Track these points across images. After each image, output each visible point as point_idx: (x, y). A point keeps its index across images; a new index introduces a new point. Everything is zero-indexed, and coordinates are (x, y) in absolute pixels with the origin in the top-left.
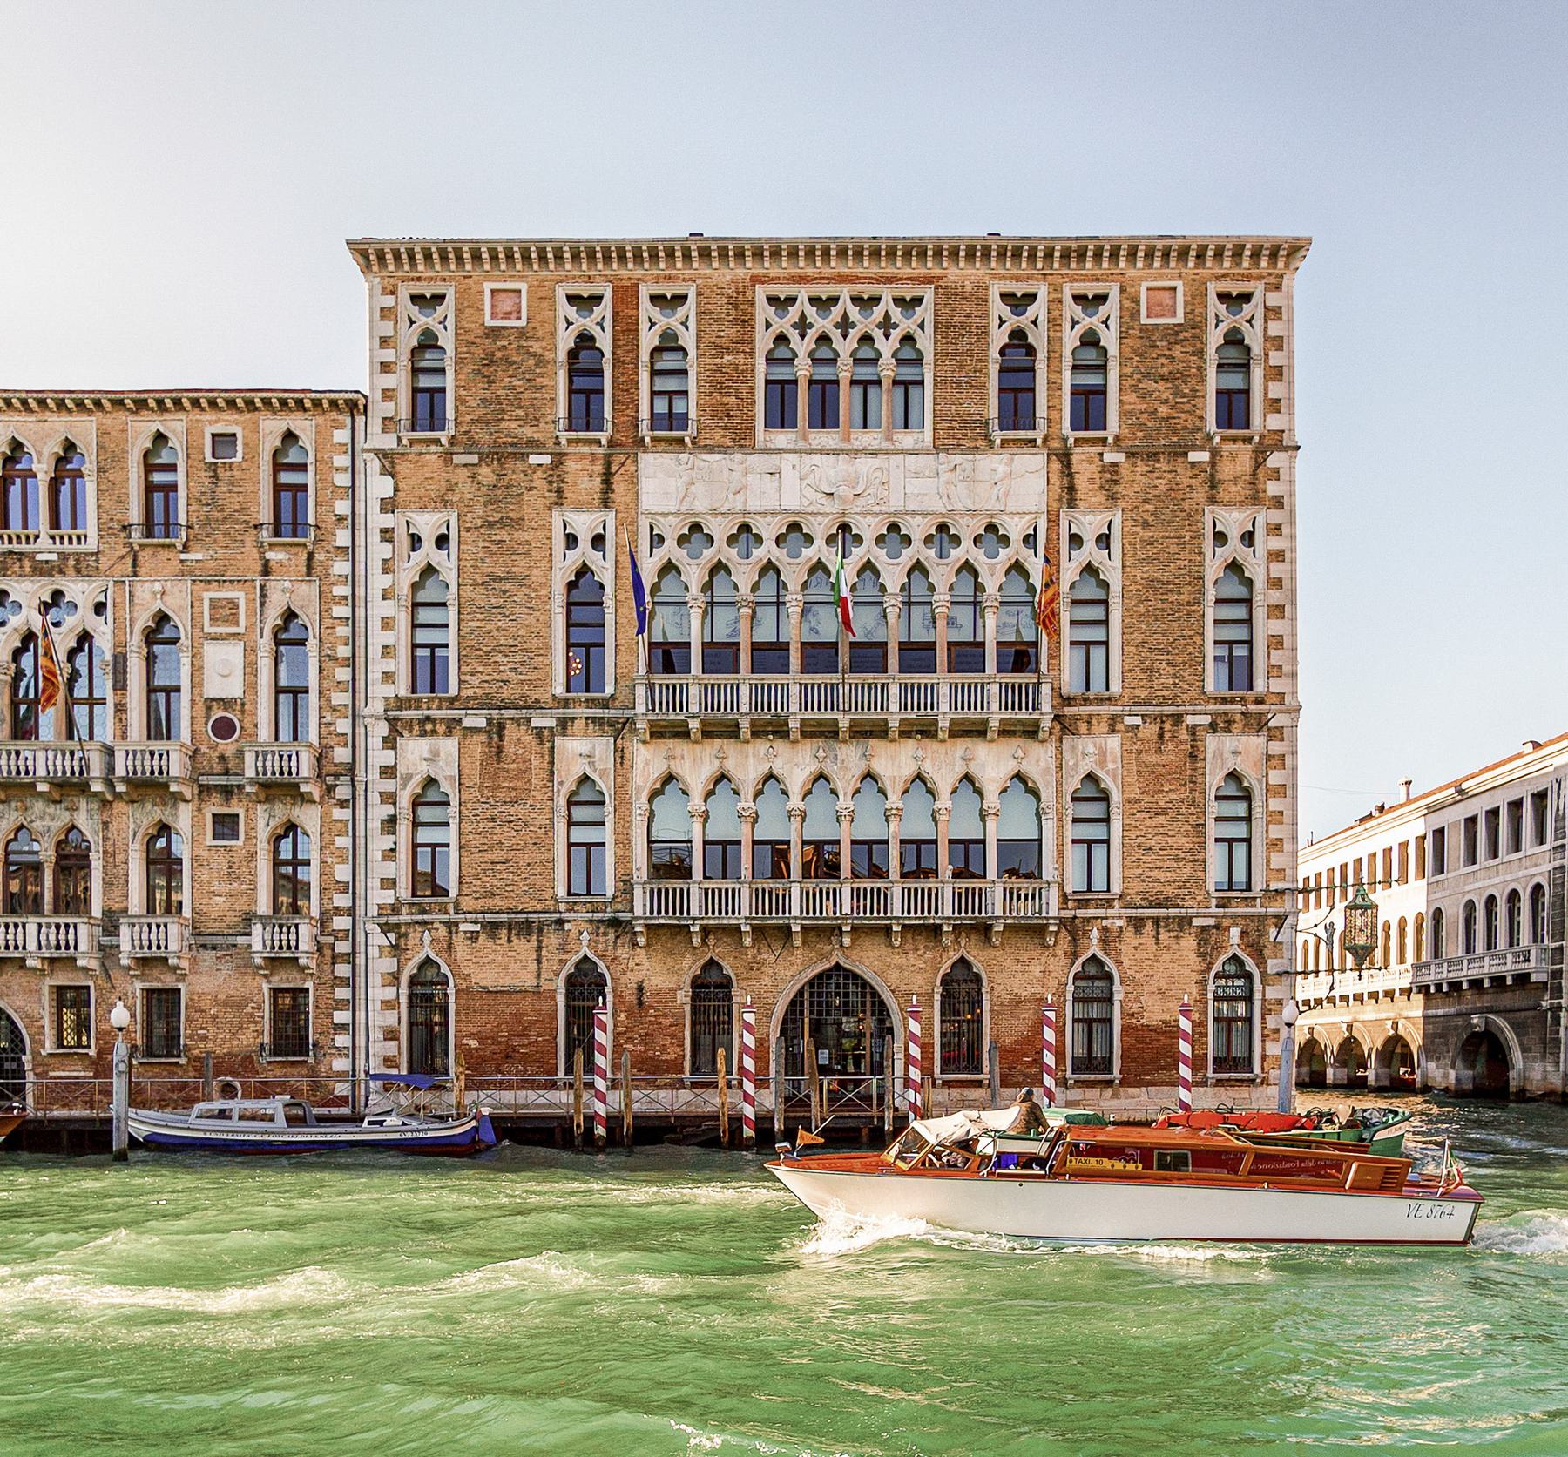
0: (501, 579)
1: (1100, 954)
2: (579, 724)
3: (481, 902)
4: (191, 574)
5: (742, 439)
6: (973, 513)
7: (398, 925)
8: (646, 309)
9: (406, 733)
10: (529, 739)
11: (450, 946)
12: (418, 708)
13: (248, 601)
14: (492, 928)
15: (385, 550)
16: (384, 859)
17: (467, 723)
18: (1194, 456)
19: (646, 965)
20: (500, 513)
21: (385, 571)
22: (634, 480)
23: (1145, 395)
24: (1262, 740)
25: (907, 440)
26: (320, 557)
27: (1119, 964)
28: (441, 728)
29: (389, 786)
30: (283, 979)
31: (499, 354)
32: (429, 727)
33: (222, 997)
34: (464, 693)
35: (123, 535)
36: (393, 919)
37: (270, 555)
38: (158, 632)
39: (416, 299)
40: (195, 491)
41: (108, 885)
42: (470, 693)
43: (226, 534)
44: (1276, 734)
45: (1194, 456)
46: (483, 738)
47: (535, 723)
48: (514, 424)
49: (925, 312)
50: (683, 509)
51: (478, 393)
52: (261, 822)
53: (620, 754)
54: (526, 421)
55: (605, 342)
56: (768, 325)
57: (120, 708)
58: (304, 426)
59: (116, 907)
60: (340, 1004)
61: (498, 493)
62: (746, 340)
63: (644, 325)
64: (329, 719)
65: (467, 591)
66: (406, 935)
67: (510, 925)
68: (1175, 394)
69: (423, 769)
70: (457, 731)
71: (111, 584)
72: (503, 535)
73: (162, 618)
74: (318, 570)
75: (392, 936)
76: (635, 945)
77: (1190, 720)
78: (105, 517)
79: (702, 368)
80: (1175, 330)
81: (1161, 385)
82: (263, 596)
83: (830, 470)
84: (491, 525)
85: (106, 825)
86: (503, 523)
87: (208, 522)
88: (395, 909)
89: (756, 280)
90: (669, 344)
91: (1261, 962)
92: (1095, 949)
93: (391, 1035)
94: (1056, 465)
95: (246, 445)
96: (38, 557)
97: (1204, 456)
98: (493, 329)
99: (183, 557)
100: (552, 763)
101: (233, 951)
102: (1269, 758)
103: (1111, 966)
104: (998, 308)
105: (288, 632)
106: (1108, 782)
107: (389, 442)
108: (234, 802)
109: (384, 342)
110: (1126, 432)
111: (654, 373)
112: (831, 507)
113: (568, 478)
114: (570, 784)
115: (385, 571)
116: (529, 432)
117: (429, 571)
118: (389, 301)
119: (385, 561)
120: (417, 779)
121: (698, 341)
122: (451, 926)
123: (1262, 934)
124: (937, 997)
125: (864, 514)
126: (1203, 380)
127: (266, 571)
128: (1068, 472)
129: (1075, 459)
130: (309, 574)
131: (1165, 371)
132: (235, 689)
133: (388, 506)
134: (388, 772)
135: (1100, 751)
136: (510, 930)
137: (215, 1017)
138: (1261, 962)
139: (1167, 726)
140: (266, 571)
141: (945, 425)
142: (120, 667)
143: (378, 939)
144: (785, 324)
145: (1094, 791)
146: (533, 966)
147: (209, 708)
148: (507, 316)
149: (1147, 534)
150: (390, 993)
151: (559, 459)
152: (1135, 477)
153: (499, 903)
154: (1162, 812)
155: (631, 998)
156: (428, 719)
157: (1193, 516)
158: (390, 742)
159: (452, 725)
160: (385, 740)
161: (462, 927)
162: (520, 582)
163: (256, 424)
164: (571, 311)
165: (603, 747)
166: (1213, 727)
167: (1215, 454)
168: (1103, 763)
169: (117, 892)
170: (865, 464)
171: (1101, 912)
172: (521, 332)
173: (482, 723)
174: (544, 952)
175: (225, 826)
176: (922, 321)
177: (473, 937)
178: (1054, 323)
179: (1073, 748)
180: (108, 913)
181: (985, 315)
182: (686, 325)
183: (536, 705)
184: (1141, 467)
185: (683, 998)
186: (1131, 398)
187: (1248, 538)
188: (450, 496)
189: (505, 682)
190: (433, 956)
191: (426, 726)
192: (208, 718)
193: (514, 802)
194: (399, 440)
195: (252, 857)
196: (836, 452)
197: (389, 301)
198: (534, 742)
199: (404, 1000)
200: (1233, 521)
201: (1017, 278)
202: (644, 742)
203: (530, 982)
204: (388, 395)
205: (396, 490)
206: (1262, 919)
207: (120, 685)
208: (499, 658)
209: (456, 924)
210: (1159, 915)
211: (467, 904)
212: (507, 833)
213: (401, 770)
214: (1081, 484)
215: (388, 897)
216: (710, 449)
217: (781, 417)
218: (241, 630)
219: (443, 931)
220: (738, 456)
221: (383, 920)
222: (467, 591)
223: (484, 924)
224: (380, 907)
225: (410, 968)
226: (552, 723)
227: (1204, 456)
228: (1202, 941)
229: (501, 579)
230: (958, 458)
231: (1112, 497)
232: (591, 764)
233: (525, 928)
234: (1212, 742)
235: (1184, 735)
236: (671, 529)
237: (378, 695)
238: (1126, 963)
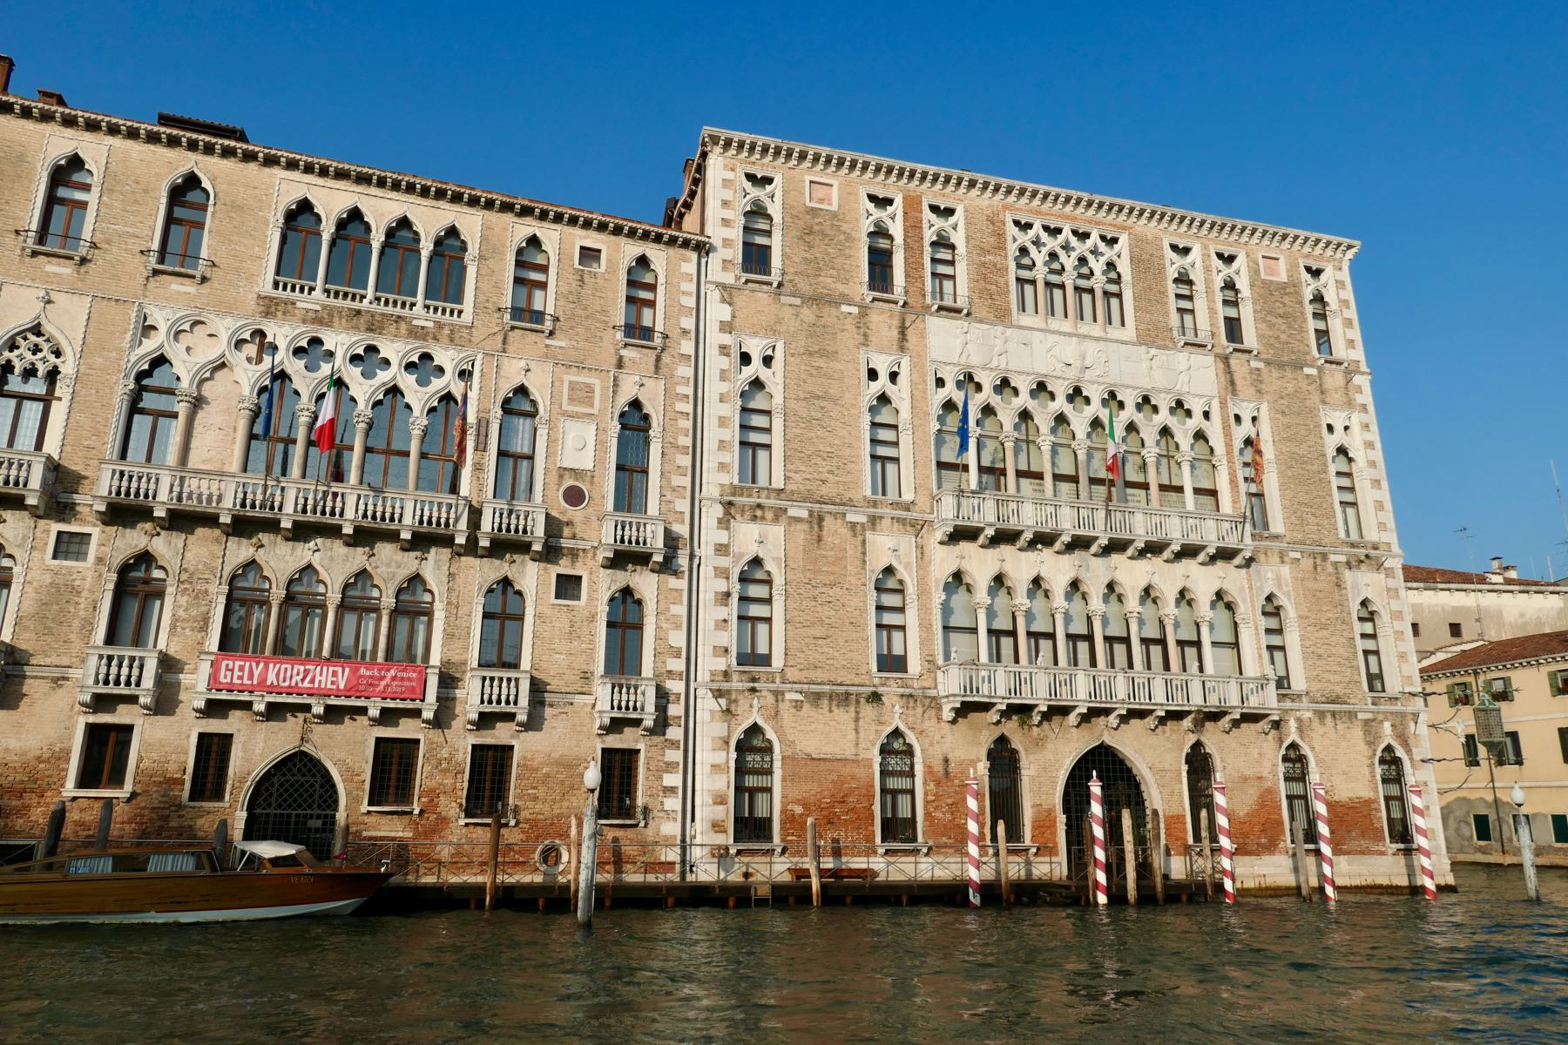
0: (819, 397)
1: (1298, 741)
2: (886, 522)
3: (804, 673)
4: (555, 357)
6: (1168, 391)
7: (729, 692)
8: (928, 215)
9: (738, 517)
10: (845, 531)
11: (777, 713)
12: (750, 496)
13: (604, 388)
14: (816, 698)
15: (724, 362)
16: (717, 627)
17: (792, 512)
18: (1307, 370)
19: (949, 738)
20: (818, 348)
21: (723, 379)
22: (922, 335)
23: (1271, 326)
24: (1383, 576)
25: (1115, 332)
26: (666, 359)
27: (1313, 749)
28: (769, 515)
29: (724, 562)
31: (816, 228)
32: (759, 513)
33: (555, 755)
34: (790, 487)
35: (497, 315)
36: (725, 686)
37: (624, 352)
38: (518, 403)
39: (750, 177)
40: (564, 289)
41: (449, 636)
42: (794, 487)
43: (587, 329)
44: (1390, 573)
45: (1307, 370)
46: (805, 526)
47: (851, 517)
48: (829, 280)
50: (963, 360)
51: (800, 253)
52: (600, 586)
53: (921, 549)
54: (837, 279)
55: (897, 229)
56: (1015, 240)
57: (478, 468)
59: (455, 659)
60: (670, 767)
61: (815, 330)
62: (1001, 247)
63: (925, 225)
64: (669, 497)
65: (792, 404)
66: (735, 701)
67: (831, 697)
68: (1290, 327)
69: (751, 551)
70: (783, 519)
71: (480, 356)
72: (821, 363)
74: (663, 370)
75: (723, 702)
76: (939, 719)
77: (1333, 558)
78: (482, 298)
79: (971, 262)
80: (1284, 286)
81: (1280, 321)
82: (616, 385)
83: (1069, 350)
84: (811, 354)
85: (451, 575)
86: (822, 353)
87: (572, 317)
88: (726, 675)
89: (1005, 208)
90: (942, 242)
91: (1409, 751)
92: (1293, 735)
93: (720, 800)
94: (1221, 365)
95: (609, 260)
96: (415, 322)
97: (1314, 372)
98: (812, 209)
99: (548, 342)
100: (864, 553)
101: (569, 709)
102: (1389, 590)
103: (1306, 749)
105: (635, 421)
106: (1282, 600)
107: (729, 278)
108: (579, 564)
109: (725, 204)
110: (1262, 349)
111: (934, 260)
112: (1072, 374)
113: (872, 326)
114: (878, 574)
115: (723, 379)
116: (841, 288)
117: (757, 384)
118: (730, 175)
119: (722, 371)
120: (749, 557)
121: (968, 242)
122: (778, 694)
123: (1406, 727)
124: (1184, 774)
125: (1093, 383)
126: (1305, 320)
127: (620, 364)
128: (1228, 370)
129: (1232, 362)
130: (656, 372)
131: (1281, 311)
132: (586, 462)
133: (726, 327)
134: (722, 549)
135: (1275, 576)
136: (831, 699)
137: (547, 776)
138: (1409, 751)
139: (1318, 561)
140: (620, 364)
141: (1142, 327)
142: (483, 431)
143: (707, 705)
144: (1025, 238)
145: (1272, 609)
146: (852, 735)
147: (561, 477)
148: (821, 201)
149: (1286, 420)
150: (720, 757)
151: (864, 310)
152: (1272, 377)
153: (819, 675)
154: (1324, 627)
155: (939, 768)
156: (759, 506)
157: (1313, 413)
158: (724, 523)
159: (779, 513)
160: (720, 521)
161: (788, 696)
162: (835, 402)
163: (618, 245)
164: (871, 206)
165: (907, 543)
166: (1349, 565)
167: (1320, 369)
168: (1280, 587)
169: (457, 644)
170: (1091, 348)
171: (1295, 705)
172: (834, 215)
173: (804, 514)
174: (861, 723)
175: (568, 586)
177: (798, 705)
178: (1207, 269)
179: (1258, 573)
180: (446, 663)
181: (1162, 257)
183: (850, 503)
184: (1275, 374)
185: (983, 767)
186: (1262, 326)
188: (778, 327)
189: (824, 482)
190: (761, 723)
191: (756, 513)
192: (560, 485)
193: (832, 585)
194: (738, 278)
195: (592, 618)
196: (1070, 335)
197: (730, 175)
198: (849, 534)
199: (732, 765)
201: (1180, 236)
202: (941, 543)
203: (849, 751)
204: (727, 243)
205: (733, 317)
206: (1403, 715)
207: (481, 447)
208: (818, 461)
209: (783, 693)
210: (1333, 708)
211: (792, 674)
212: (827, 611)
213: (735, 549)
214: (1238, 378)
215: (721, 664)
216: (981, 321)
218: (595, 411)
219: (770, 699)
220: (1000, 328)
221: (716, 686)
222: (792, 404)
223: (807, 694)
224: (713, 674)
225: (738, 733)
226: (863, 519)
227: (1314, 372)
228: (1367, 733)
229: (819, 397)
230: (1153, 351)
231: (1259, 391)
232: (898, 557)
233: (844, 699)
235: (1330, 569)
237: (715, 481)
238: (1317, 748)
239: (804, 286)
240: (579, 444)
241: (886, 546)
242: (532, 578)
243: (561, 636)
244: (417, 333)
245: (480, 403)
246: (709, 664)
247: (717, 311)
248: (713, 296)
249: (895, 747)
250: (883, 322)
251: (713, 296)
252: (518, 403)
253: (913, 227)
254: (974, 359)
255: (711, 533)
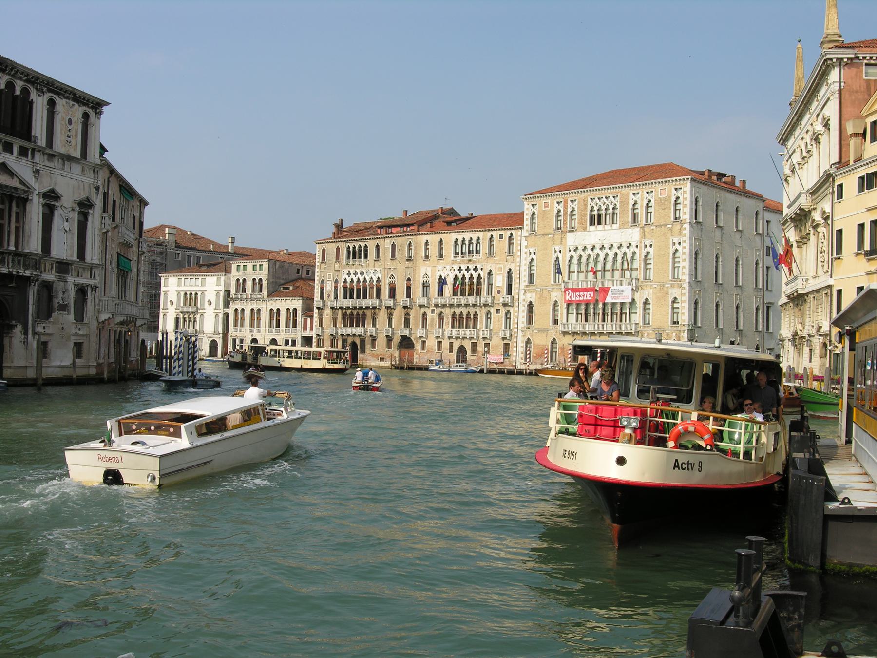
5: (585, 229)
25: (615, 226)
30: (506, 342)
38: (490, 274)
49: (618, 199)
52: (503, 311)
58: (513, 232)
73: (491, 271)
80: (665, 198)
104: (632, 196)
107: (527, 234)
133: (526, 247)
134: (524, 300)
158: (524, 294)
175: (498, 311)
176: (617, 202)
182: (575, 205)
184: (659, 229)
187: (679, 243)
200: (676, 240)
215: (523, 325)
217: (592, 223)
234: (670, 291)
236: (572, 249)
239: (542, 233)
240: (500, 281)
241: (556, 295)
242: (493, 311)
243: (498, 320)
244: (474, 262)
245: (484, 275)
246: (521, 325)
247: (524, 243)
248: (523, 239)
249: (554, 342)
250: (558, 236)
251: (523, 239)
252: (490, 274)
253: (566, 207)
254: (577, 244)
255: (522, 297)
